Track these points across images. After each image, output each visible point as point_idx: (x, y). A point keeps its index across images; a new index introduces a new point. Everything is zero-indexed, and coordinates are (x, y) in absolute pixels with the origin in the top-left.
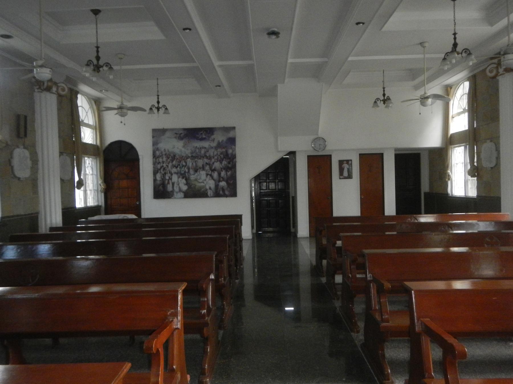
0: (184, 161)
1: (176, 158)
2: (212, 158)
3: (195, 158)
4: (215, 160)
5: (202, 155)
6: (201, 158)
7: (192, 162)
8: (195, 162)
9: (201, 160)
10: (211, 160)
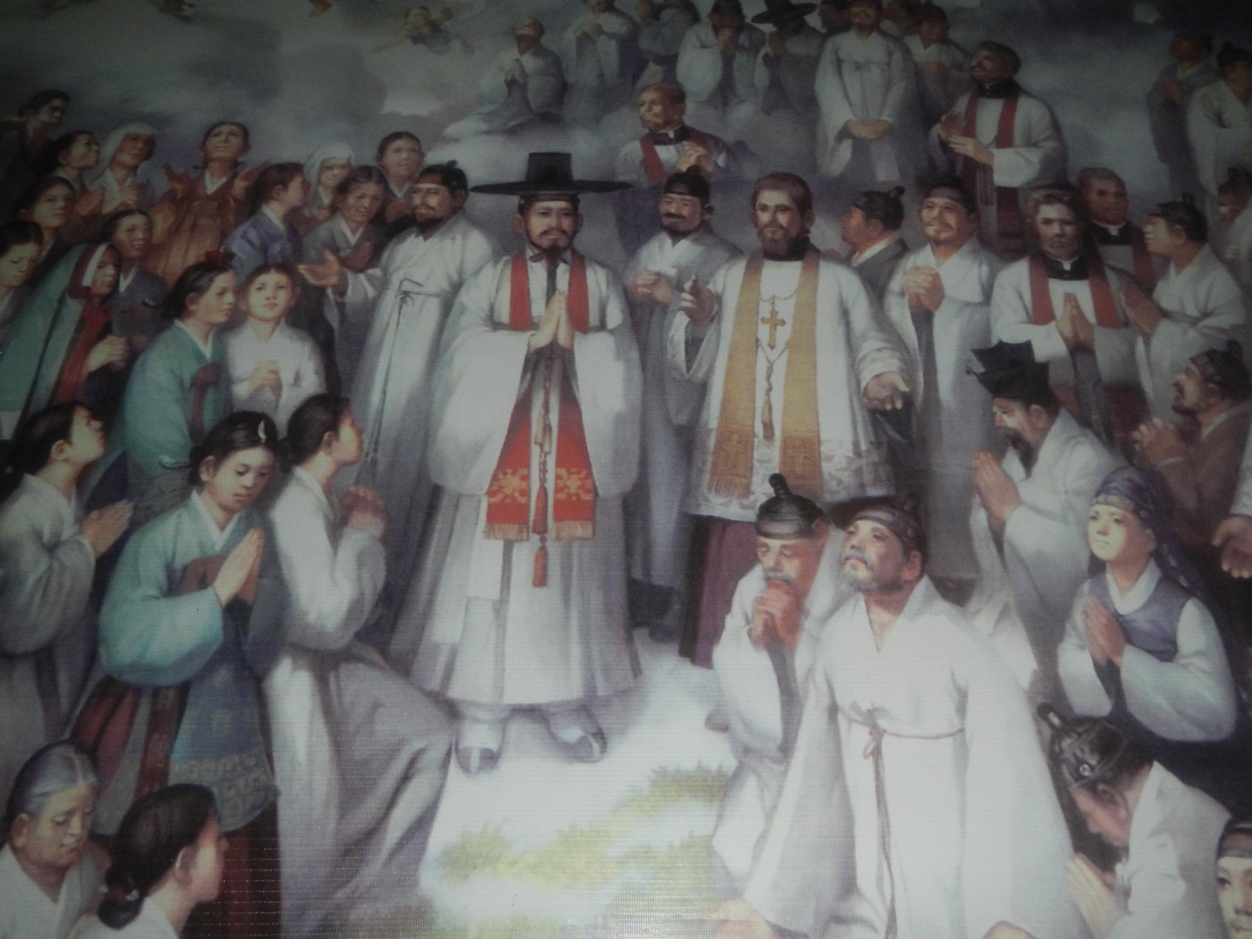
1: (48, 212)
2: (1159, 235)
5: (840, 159)
6: (823, 232)
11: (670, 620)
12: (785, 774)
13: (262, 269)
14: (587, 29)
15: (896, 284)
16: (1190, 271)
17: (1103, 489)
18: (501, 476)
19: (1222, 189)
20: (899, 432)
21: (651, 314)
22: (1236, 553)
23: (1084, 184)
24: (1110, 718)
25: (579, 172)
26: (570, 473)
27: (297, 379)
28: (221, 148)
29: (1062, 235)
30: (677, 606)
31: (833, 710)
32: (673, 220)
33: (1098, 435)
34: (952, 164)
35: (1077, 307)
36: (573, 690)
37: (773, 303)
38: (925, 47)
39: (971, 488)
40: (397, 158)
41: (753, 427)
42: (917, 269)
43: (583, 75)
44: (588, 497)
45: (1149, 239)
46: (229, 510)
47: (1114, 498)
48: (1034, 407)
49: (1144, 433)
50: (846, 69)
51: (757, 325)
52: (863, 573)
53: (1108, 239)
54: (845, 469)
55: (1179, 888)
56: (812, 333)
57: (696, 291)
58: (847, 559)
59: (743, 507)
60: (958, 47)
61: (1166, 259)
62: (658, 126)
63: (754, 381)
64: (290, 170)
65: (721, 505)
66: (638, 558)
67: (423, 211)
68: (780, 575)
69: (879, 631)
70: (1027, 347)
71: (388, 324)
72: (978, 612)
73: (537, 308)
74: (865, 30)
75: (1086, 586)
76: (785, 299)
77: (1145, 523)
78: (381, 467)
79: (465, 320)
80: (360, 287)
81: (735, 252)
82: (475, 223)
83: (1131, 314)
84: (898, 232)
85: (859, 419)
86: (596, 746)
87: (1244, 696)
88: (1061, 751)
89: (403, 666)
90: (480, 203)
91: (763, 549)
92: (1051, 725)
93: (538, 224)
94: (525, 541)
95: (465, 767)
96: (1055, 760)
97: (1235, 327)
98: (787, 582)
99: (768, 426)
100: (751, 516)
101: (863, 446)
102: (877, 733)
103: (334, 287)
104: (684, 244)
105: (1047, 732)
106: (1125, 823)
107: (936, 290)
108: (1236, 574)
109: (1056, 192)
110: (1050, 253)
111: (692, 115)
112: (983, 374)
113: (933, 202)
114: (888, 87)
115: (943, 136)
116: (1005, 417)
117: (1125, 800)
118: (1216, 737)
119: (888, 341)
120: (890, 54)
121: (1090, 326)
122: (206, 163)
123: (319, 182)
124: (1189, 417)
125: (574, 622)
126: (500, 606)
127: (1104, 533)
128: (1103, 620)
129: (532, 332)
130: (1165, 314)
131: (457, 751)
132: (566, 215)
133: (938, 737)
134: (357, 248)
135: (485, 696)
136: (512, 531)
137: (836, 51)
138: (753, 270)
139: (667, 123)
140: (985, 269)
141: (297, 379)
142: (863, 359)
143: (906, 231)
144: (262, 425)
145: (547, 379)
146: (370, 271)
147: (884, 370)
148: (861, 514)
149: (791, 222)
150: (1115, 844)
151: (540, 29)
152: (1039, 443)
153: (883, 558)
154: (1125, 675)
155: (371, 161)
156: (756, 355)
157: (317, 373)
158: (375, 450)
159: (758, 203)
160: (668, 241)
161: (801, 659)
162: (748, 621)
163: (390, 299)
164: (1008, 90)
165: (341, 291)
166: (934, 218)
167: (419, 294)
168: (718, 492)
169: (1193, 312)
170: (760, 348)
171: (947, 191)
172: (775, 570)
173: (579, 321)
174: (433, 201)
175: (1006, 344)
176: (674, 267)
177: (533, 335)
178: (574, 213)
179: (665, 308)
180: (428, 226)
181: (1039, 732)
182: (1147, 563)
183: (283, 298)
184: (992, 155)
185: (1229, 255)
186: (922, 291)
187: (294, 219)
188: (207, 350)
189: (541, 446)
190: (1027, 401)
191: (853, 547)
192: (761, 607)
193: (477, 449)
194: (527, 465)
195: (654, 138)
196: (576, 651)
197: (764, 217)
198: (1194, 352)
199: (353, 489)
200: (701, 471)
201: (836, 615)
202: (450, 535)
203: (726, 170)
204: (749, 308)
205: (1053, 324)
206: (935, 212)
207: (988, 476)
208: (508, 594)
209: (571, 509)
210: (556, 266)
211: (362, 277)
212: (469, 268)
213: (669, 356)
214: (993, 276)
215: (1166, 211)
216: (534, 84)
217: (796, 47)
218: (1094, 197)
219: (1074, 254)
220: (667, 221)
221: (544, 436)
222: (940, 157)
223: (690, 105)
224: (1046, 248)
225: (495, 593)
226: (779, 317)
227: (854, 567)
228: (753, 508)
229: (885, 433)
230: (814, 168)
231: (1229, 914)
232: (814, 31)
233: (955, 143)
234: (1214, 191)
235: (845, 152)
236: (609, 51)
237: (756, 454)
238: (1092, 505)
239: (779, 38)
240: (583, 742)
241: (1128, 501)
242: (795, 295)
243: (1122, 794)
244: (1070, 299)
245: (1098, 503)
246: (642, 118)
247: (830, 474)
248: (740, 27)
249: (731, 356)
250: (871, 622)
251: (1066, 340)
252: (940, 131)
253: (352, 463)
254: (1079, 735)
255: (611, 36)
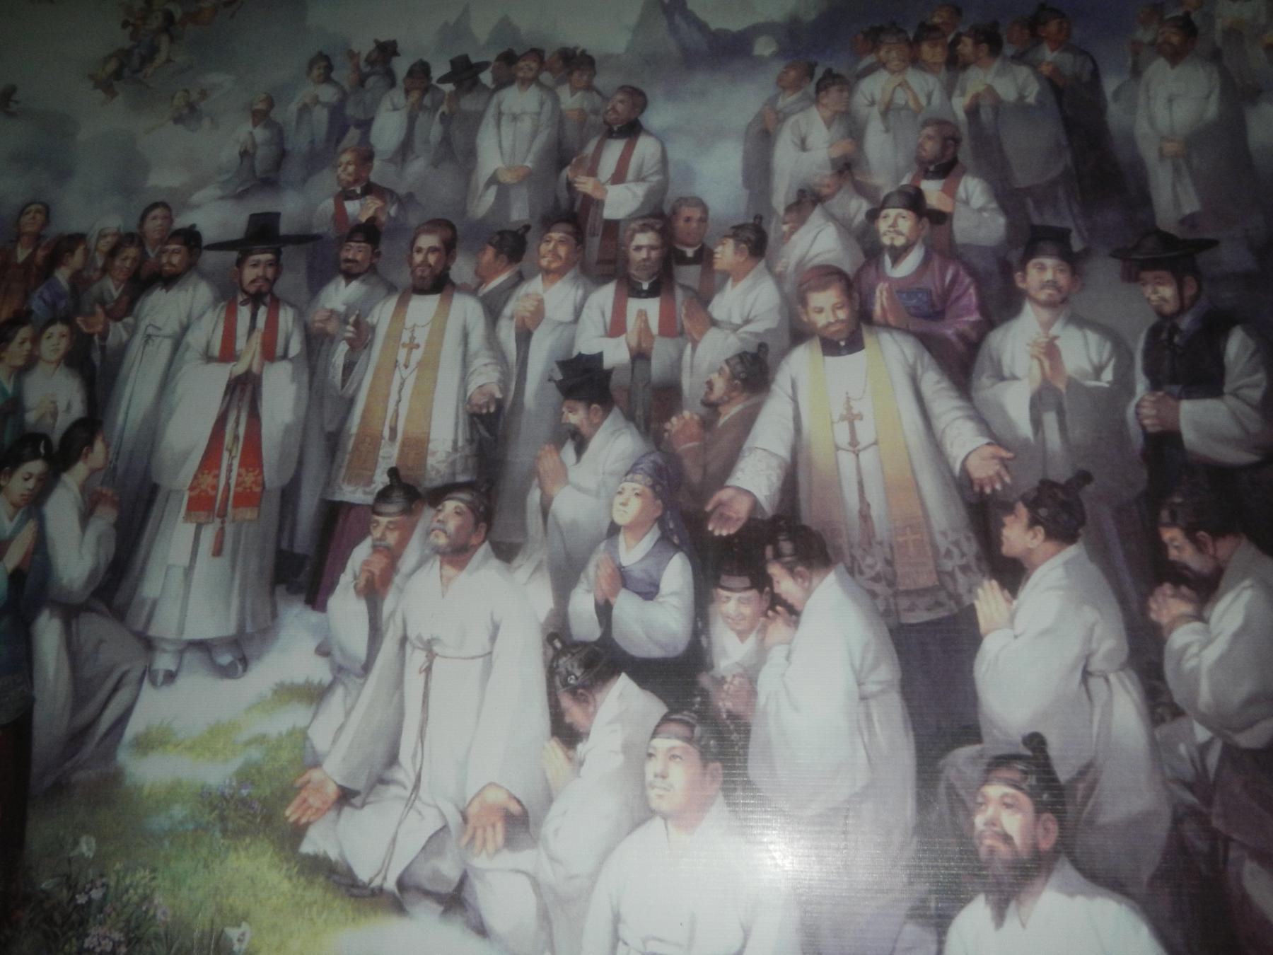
0: (55, 341)
2: (726, 254)
3: (318, 279)
4: (793, 304)
5: (484, 203)
6: (461, 269)
7: (249, 350)
8: (316, 342)
9: (466, 309)
10: (703, 298)
11: (303, 578)
12: (363, 685)
13: (51, 322)
14: (307, 100)
15: (508, 311)
16: (744, 284)
17: (632, 470)
18: (200, 476)
19: (789, 209)
20: (488, 430)
21: (322, 344)
22: (722, 515)
23: (675, 212)
24: (596, 643)
25: (285, 228)
26: (247, 471)
27: (69, 406)
28: (29, 224)
29: (648, 259)
30: (308, 568)
31: (404, 640)
32: (349, 265)
33: (638, 427)
34: (572, 204)
35: (646, 321)
36: (230, 629)
37: (413, 330)
38: (573, 94)
39: (533, 473)
40: (153, 225)
41: (382, 431)
42: (527, 295)
43: (298, 142)
44: (257, 489)
45: (717, 258)
46: (16, 506)
47: (639, 477)
48: (595, 406)
49: (674, 423)
50: (504, 120)
51: (398, 348)
52: (442, 541)
53: (683, 260)
54: (444, 462)
55: (620, 759)
56: (438, 353)
57: (357, 324)
58: (433, 530)
59: (365, 493)
60: (599, 93)
61: (726, 275)
62: (350, 184)
63: (388, 395)
64: (78, 238)
65: (350, 492)
66: (286, 534)
67: (167, 268)
68: (383, 543)
69: (445, 582)
70: (599, 357)
71: (134, 361)
72: (519, 567)
73: (240, 344)
74: (526, 83)
75: (602, 546)
76: (423, 326)
77: (657, 495)
78: (120, 471)
79: (188, 355)
80: (117, 332)
81: (391, 288)
82: (203, 276)
83: (687, 324)
84: (519, 264)
85: (461, 421)
86: (240, 667)
87: (700, 625)
88: (558, 666)
89: (120, 614)
90: (210, 259)
91: (375, 525)
92: (555, 648)
93: (249, 273)
94: (211, 523)
95: (153, 683)
96: (552, 672)
97: (768, 331)
98: (388, 548)
99: (393, 431)
100: (369, 500)
101: (460, 444)
102: (431, 655)
103: (99, 334)
104: (355, 284)
105: (551, 652)
106: (591, 717)
107: (539, 313)
108: (717, 533)
109: (652, 221)
110: (634, 276)
111: (379, 172)
112: (560, 381)
113: (551, 237)
114: (534, 134)
115: (570, 175)
116: (570, 415)
117: (595, 700)
118: (671, 654)
119: (494, 358)
120: (542, 104)
121: (652, 337)
122: (18, 238)
123: (96, 249)
124: (713, 407)
125: (237, 582)
126: (189, 571)
127: (624, 504)
128: (609, 571)
129: (233, 364)
130: (714, 323)
131: (149, 671)
132: (271, 265)
133: (473, 658)
134: (118, 301)
135: (171, 633)
136: (202, 515)
137: (499, 105)
138: (403, 304)
139: (356, 181)
140: (580, 292)
141: (69, 406)
142: (472, 373)
143: (525, 264)
144: (42, 444)
145: (240, 400)
146: (126, 320)
147: (486, 382)
148: (449, 496)
149: (436, 263)
150: (581, 730)
151: (271, 103)
152: (591, 436)
153: (459, 529)
154: (616, 612)
155: (133, 227)
156: (393, 374)
157: (82, 402)
158: (117, 459)
159: (415, 246)
160: (343, 283)
161: (388, 605)
162: (355, 578)
163: (138, 340)
164: (631, 129)
165: (104, 337)
166: (549, 251)
167: (158, 336)
168: (349, 482)
169: (737, 320)
170: (397, 369)
171: (564, 226)
172: (377, 540)
173: (269, 354)
174: (176, 259)
175: (583, 355)
176: (345, 304)
177: (234, 366)
178: (276, 264)
179: (332, 339)
180: (169, 280)
181: (545, 653)
182: (652, 526)
183: (64, 344)
184: (606, 192)
185: (779, 268)
186: (528, 314)
187: (78, 281)
188: (9, 388)
189: (230, 451)
190: (589, 401)
191: (439, 521)
192: (366, 568)
193: (186, 455)
194: (219, 467)
195: (347, 195)
196: (235, 602)
197: (418, 258)
198: (730, 353)
199: (99, 488)
200: (341, 467)
201: (418, 572)
202: (161, 521)
203: (395, 219)
204: (394, 337)
205: (622, 338)
206: (551, 246)
207: (547, 463)
208: (195, 562)
209: (246, 498)
210: (258, 309)
211: (119, 325)
212: (196, 312)
213: (330, 378)
214: (585, 298)
215: (737, 232)
216: (260, 152)
217: (469, 103)
218: (681, 224)
219: (651, 278)
220: (344, 266)
221: (233, 444)
222: (564, 195)
223: (376, 163)
224: (633, 271)
225: (185, 560)
226: (416, 342)
227: (437, 536)
228: (372, 494)
229: (478, 431)
230: (464, 212)
231: (649, 777)
232: (485, 86)
233: (580, 183)
234: (781, 210)
235: (490, 197)
236: (321, 116)
237: (382, 453)
238: (621, 483)
239: (456, 96)
240: (232, 664)
241: (649, 479)
242: (430, 324)
243: (593, 696)
244: (642, 315)
245: (625, 481)
246: (338, 177)
247: (432, 466)
248: (426, 89)
249: (375, 376)
250: (441, 576)
251: (630, 349)
252: (569, 173)
253: (99, 470)
254: (573, 655)
255: (324, 105)
